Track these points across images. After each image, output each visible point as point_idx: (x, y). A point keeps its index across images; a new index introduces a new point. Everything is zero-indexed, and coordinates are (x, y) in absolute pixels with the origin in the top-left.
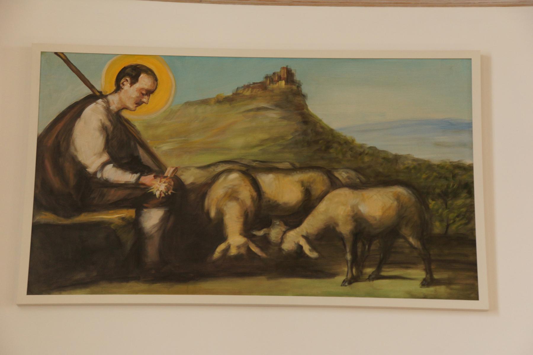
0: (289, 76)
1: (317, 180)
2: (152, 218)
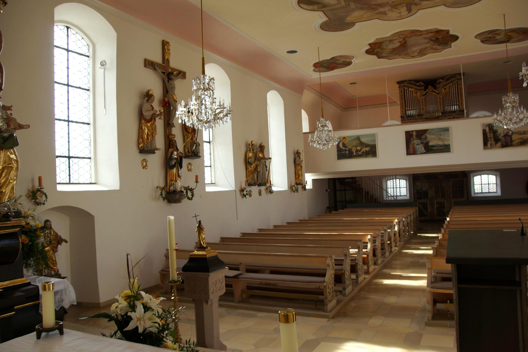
2: (347, 152)
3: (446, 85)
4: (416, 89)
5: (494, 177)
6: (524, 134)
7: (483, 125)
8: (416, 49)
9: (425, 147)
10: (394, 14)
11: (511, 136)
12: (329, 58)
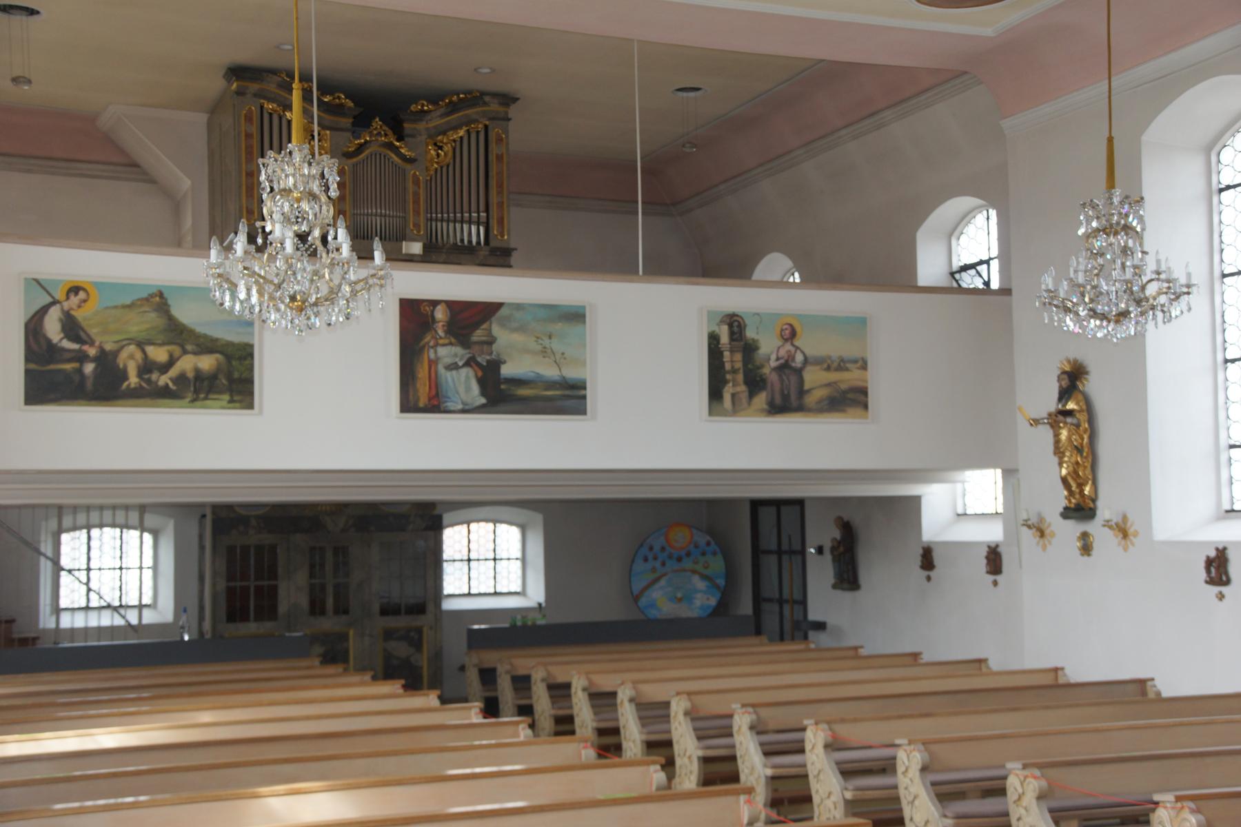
0: (161, 294)
1: (177, 350)
2: (89, 368)
3: (444, 133)
6: (840, 368)
7: (711, 314)
9: (482, 382)
11: (799, 372)
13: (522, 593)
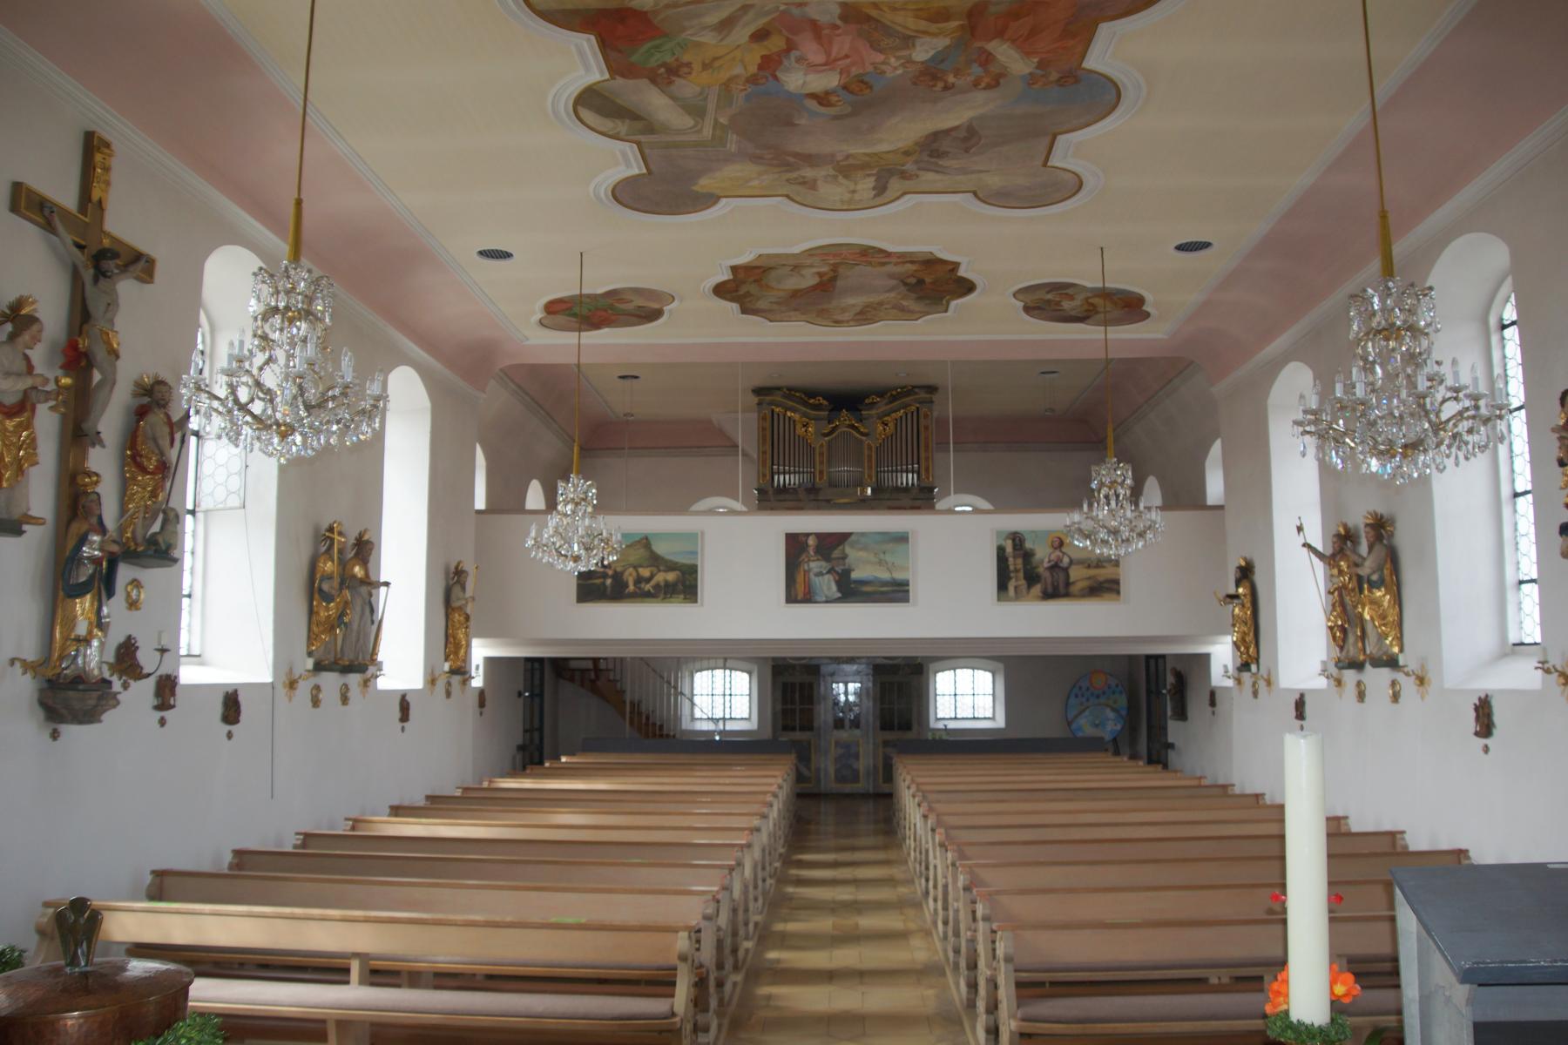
2: (609, 581)
4: (804, 415)
5: (988, 676)
6: (1097, 566)
7: (999, 533)
8: (856, 301)
9: (838, 583)
10: (833, 191)
11: (1066, 570)
12: (601, 291)
13: (993, 719)
